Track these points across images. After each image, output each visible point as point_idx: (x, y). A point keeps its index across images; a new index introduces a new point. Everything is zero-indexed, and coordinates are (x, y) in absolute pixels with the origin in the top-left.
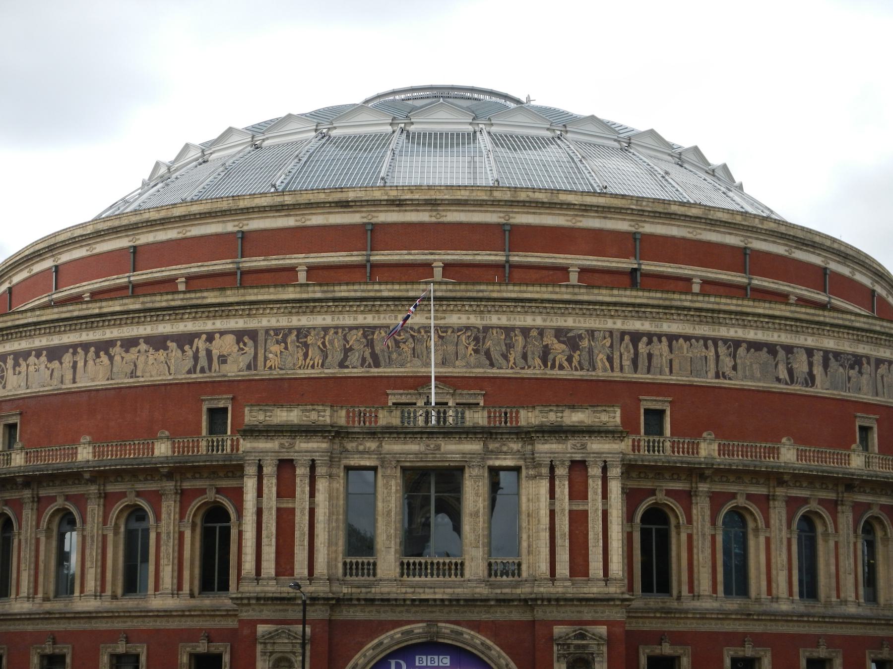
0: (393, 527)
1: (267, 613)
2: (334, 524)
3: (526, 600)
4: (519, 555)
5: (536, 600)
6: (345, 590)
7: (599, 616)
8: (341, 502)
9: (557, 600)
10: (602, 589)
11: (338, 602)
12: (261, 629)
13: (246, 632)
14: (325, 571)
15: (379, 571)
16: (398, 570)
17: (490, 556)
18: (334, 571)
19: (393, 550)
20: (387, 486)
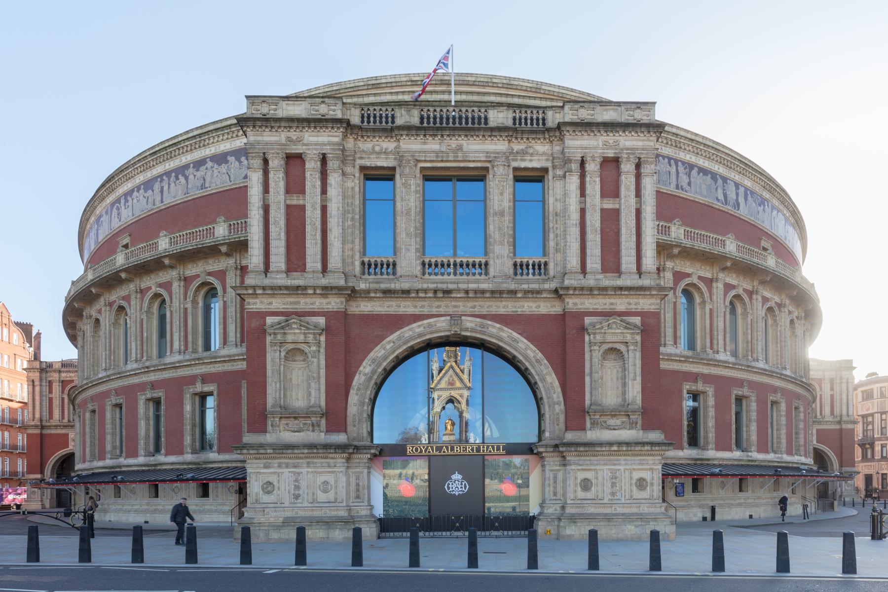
0: (413, 225)
1: (277, 304)
2: (350, 223)
3: (556, 291)
4: (545, 254)
5: (567, 288)
6: (363, 286)
7: (633, 308)
8: (357, 202)
9: (591, 289)
10: (635, 282)
11: (353, 294)
12: (270, 320)
13: (255, 324)
14: (340, 265)
15: (398, 269)
16: (419, 268)
17: (515, 255)
18: (351, 268)
19: (413, 248)
20: (406, 185)
